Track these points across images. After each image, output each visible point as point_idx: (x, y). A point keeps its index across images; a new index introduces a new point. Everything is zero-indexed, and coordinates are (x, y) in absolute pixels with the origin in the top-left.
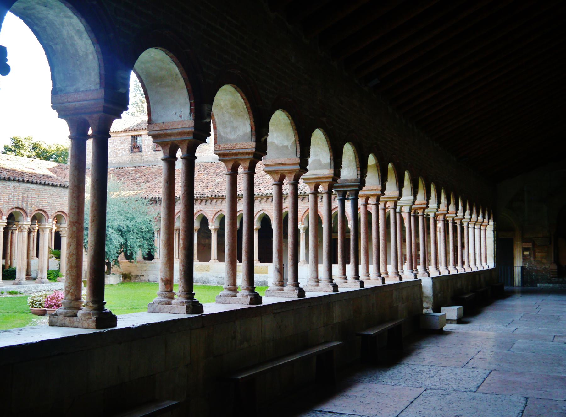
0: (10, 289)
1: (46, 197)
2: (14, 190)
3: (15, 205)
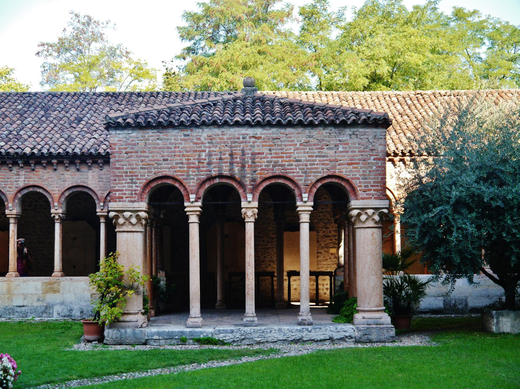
0: (201, 333)
1: (291, 149)
2: (209, 143)
3: (214, 171)
